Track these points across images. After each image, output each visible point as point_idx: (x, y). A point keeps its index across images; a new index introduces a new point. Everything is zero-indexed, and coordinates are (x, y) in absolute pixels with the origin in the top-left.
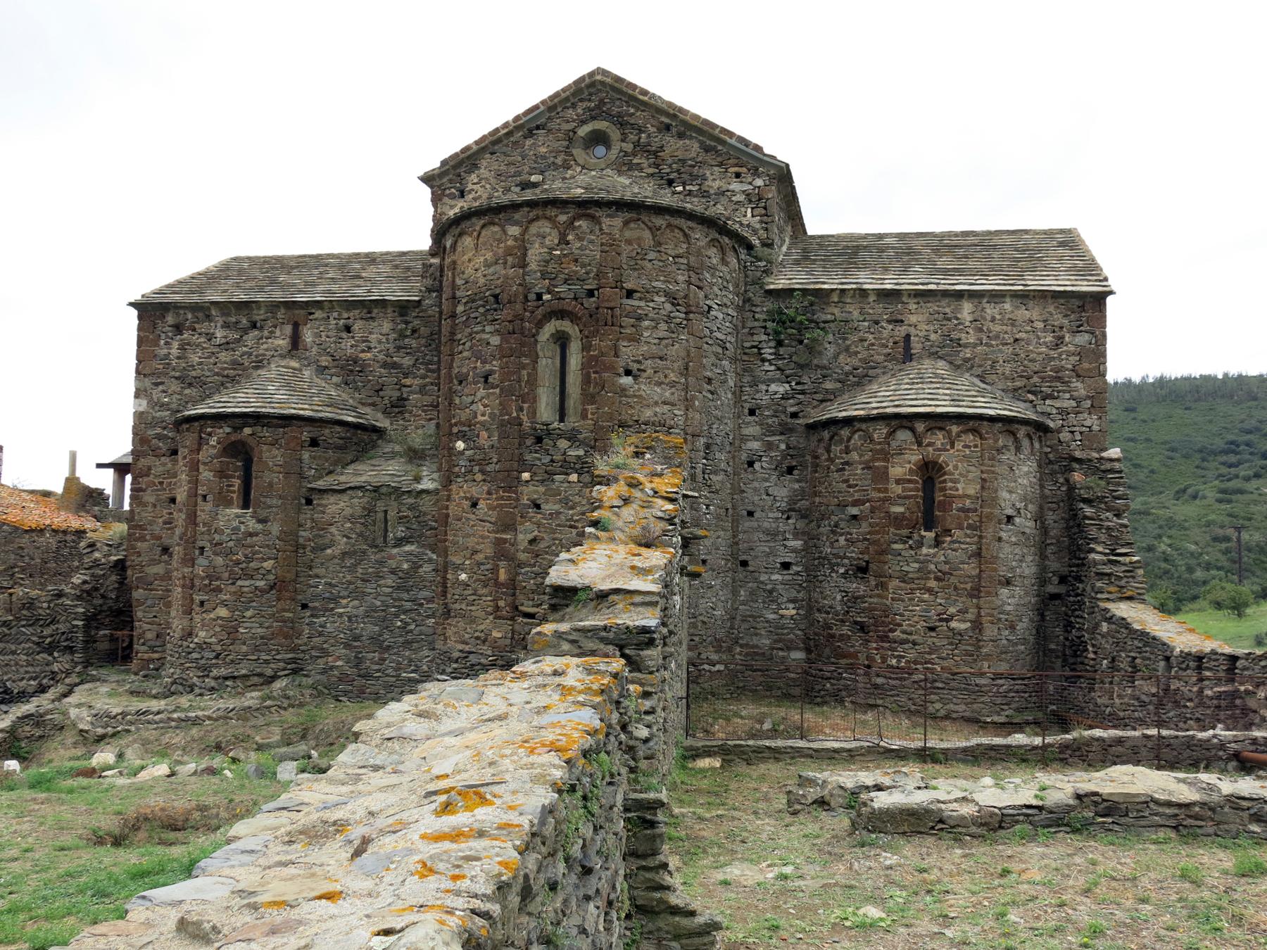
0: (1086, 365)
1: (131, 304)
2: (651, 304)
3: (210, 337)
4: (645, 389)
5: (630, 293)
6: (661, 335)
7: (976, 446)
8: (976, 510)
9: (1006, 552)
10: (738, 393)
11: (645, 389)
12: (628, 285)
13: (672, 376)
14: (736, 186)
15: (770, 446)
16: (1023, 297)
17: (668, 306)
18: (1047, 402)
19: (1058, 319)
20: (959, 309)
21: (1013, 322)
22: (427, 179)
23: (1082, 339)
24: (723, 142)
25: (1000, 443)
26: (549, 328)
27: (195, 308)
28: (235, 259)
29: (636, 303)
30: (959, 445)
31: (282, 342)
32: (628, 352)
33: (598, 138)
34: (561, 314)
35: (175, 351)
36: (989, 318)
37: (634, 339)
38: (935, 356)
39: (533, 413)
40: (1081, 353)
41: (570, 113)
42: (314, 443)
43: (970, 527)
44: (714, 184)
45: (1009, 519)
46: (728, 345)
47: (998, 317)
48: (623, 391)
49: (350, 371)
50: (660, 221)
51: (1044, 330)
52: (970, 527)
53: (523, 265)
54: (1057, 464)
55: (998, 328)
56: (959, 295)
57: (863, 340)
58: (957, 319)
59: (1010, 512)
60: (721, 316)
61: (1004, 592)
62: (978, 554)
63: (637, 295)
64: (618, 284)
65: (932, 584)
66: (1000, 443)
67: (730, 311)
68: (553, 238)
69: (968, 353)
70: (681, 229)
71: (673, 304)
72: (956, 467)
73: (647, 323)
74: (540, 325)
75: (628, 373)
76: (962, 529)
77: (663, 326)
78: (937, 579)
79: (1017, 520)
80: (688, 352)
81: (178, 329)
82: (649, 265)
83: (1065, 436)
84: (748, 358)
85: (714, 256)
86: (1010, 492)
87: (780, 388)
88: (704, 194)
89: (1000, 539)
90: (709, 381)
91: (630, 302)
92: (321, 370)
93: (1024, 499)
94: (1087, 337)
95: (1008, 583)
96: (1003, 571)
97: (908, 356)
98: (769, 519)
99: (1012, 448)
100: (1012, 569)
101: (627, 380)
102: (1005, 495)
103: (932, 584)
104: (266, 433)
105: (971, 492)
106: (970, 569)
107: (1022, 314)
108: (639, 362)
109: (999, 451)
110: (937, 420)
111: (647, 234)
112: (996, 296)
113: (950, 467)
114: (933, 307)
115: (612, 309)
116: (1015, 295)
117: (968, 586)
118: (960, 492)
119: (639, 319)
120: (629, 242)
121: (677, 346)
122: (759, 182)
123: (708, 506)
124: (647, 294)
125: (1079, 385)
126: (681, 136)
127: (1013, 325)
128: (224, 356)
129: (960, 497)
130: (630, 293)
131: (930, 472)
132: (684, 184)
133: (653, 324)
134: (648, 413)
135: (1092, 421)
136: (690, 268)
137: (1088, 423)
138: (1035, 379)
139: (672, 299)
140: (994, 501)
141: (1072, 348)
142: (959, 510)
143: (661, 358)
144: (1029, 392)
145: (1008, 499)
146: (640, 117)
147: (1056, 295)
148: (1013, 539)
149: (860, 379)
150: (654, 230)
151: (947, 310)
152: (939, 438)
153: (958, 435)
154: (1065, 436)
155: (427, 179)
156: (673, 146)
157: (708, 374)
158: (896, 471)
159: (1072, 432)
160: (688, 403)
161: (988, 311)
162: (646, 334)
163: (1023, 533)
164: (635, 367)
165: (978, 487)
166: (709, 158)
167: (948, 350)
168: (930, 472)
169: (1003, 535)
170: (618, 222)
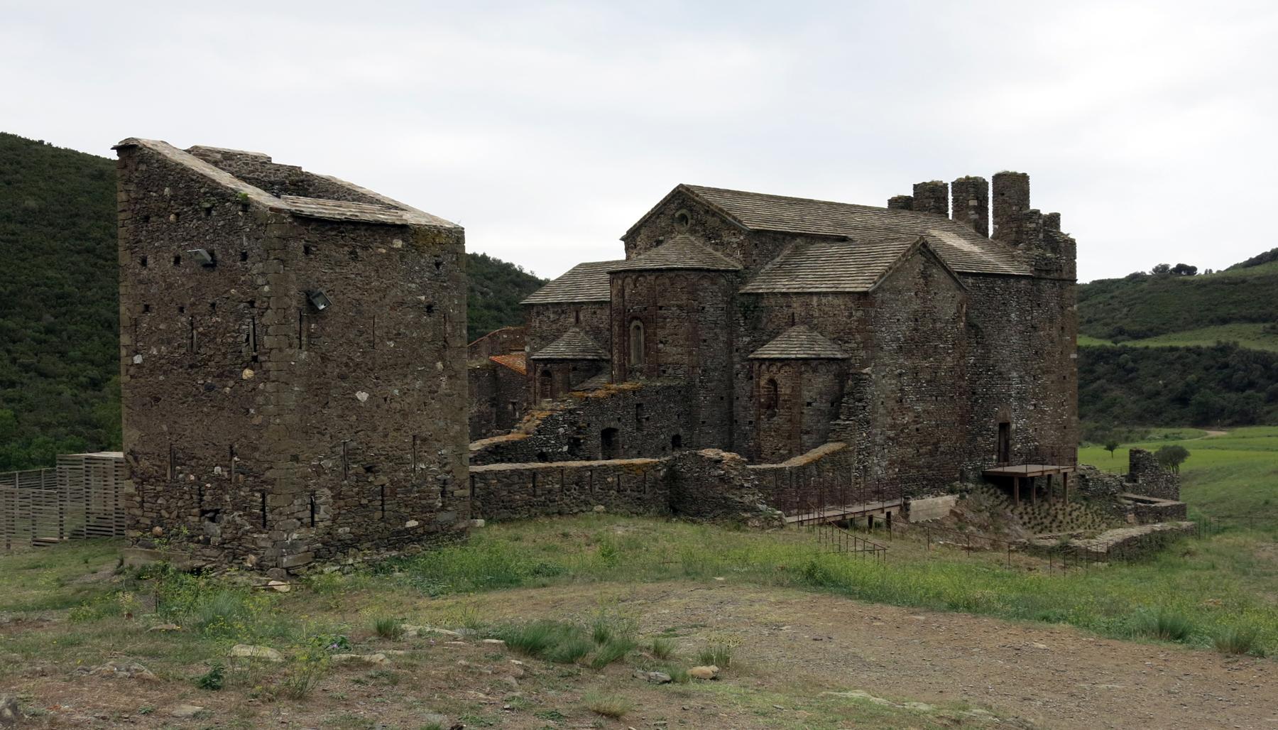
4: (668, 349)
5: (661, 308)
9: (806, 419)
10: (730, 343)
11: (668, 349)
14: (734, 240)
15: (743, 367)
16: (835, 294)
19: (850, 304)
21: (832, 306)
22: (622, 239)
23: (859, 313)
26: (635, 323)
27: (543, 305)
28: (581, 265)
31: (572, 320)
32: (661, 333)
33: (683, 218)
34: (637, 318)
37: (663, 328)
38: (803, 323)
39: (629, 361)
41: (672, 206)
42: (575, 369)
44: (726, 239)
45: (809, 404)
48: (658, 351)
49: (596, 332)
50: (672, 274)
53: (623, 296)
54: (842, 377)
56: (811, 294)
61: (805, 437)
62: (790, 420)
64: (655, 304)
68: (632, 286)
69: (815, 321)
74: (630, 322)
81: (538, 313)
83: (853, 361)
84: (731, 327)
85: (706, 283)
87: (747, 339)
88: (722, 244)
92: (587, 332)
93: (820, 394)
95: (807, 433)
96: (804, 427)
97: (793, 324)
98: (744, 401)
101: (661, 346)
104: (555, 366)
106: (786, 427)
107: (836, 302)
109: (801, 373)
110: (773, 361)
111: (667, 281)
112: (826, 294)
114: (802, 299)
116: (833, 293)
124: (668, 307)
126: (714, 214)
128: (554, 326)
130: (661, 308)
131: (772, 381)
135: (863, 353)
139: (680, 307)
145: (807, 395)
146: (698, 207)
147: (849, 293)
149: (773, 335)
152: (774, 369)
154: (853, 361)
155: (622, 239)
156: (712, 221)
158: (763, 383)
160: (690, 353)
166: (723, 226)
167: (808, 321)
168: (772, 381)
170: (653, 277)
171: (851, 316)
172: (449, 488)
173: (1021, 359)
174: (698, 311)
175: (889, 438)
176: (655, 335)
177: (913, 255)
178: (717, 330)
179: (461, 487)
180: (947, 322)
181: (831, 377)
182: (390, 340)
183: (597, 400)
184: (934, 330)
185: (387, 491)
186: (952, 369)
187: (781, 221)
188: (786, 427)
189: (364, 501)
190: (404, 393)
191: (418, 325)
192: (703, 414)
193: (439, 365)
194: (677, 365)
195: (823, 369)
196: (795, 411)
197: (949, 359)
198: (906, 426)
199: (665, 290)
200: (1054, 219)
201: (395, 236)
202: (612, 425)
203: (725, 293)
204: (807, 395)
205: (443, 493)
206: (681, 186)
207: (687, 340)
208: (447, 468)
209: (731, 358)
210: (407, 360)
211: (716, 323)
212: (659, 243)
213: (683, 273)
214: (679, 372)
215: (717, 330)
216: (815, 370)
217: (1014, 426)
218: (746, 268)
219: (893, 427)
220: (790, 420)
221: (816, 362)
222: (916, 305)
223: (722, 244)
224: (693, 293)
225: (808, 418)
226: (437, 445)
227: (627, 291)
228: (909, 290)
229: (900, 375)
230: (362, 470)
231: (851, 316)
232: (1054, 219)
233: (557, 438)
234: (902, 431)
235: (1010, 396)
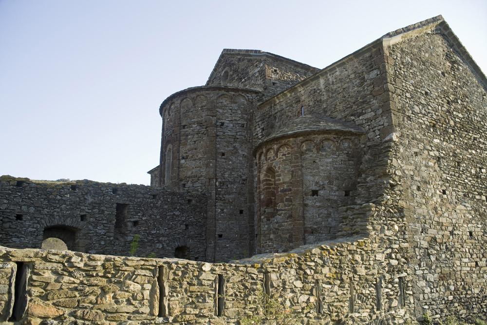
0: (377, 88)
1: (149, 173)
2: (191, 129)
5: (184, 127)
6: (195, 140)
7: (289, 154)
8: (290, 190)
9: (311, 213)
12: (183, 124)
13: (200, 156)
14: (256, 70)
17: (198, 128)
18: (361, 118)
23: (373, 74)
24: (250, 56)
25: (304, 148)
29: (185, 130)
30: (280, 155)
32: (183, 150)
36: (331, 83)
40: (373, 83)
43: (287, 200)
45: (315, 193)
46: (238, 137)
47: (334, 81)
48: (180, 166)
50: (194, 95)
51: (355, 78)
52: (287, 200)
55: (335, 87)
57: (287, 116)
58: (319, 89)
59: (314, 188)
60: (232, 125)
62: (290, 216)
63: (186, 127)
65: (272, 236)
66: (304, 148)
67: (239, 122)
70: (203, 95)
71: (201, 126)
72: (279, 168)
73: (190, 137)
75: (183, 158)
76: (283, 202)
77: (196, 136)
78: (274, 233)
79: (321, 192)
80: (206, 144)
82: (191, 113)
83: (371, 135)
85: (225, 101)
86: (313, 176)
89: (306, 205)
90: (223, 154)
91: (184, 130)
94: (375, 72)
96: (308, 224)
99: (314, 150)
100: (316, 223)
101: (183, 161)
102: (309, 178)
103: (272, 236)
105: (287, 180)
106: (287, 225)
108: (187, 153)
109: (302, 153)
113: (277, 168)
115: (177, 135)
117: (287, 236)
118: (281, 181)
119: (187, 136)
120: (183, 107)
121: (202, 142)
122: (262, 65)
123: (222, 210)
125: (374, 101)
127: (341, 82)
129: (281, 184)
130: (184, 127)
132: (244, 78)
133: (192, 136)
134: (189, 173)
136: (208, 109)
137: (381, 123)
138: (354, 107)
139: (200, 124)
140: (301, 182)
141: (369, 82)
142: (282, 191)
143: (196, 149)
144: (352, 115)
148: (318, 204)
150: (193, 99)
151: (315, 87)
153: (278, 149)
157: (223, 151)
159: (374, 131)
160: (207, 165)
161: (330, 80)
162: (189, 141)
163: (329, 200)
164: (185, 155)
165: (290, 176)
169: (309, 202)
174: (217, 126)
176: (178, 152)
178: (237, 145)
181: (343, 157)
188: (287, 225)
192: (221, 227)
194: (196, 178)
195: (329, 145)
196: (297, 202)
199: (187, 111)
203: (245, 111)
204: (311, 181)
206: (224, 50)
207: (205, 153)
209: (252, 172)
211: (235, 139)
213: (204, 92)
214: (197, 184)
215: (237, 145)
216: (320, 148)
218: (265, 89)
220: (290, 216)
221: (320, 137)
223: (249, 78)
224: (212, 109)
225: (314, 212)
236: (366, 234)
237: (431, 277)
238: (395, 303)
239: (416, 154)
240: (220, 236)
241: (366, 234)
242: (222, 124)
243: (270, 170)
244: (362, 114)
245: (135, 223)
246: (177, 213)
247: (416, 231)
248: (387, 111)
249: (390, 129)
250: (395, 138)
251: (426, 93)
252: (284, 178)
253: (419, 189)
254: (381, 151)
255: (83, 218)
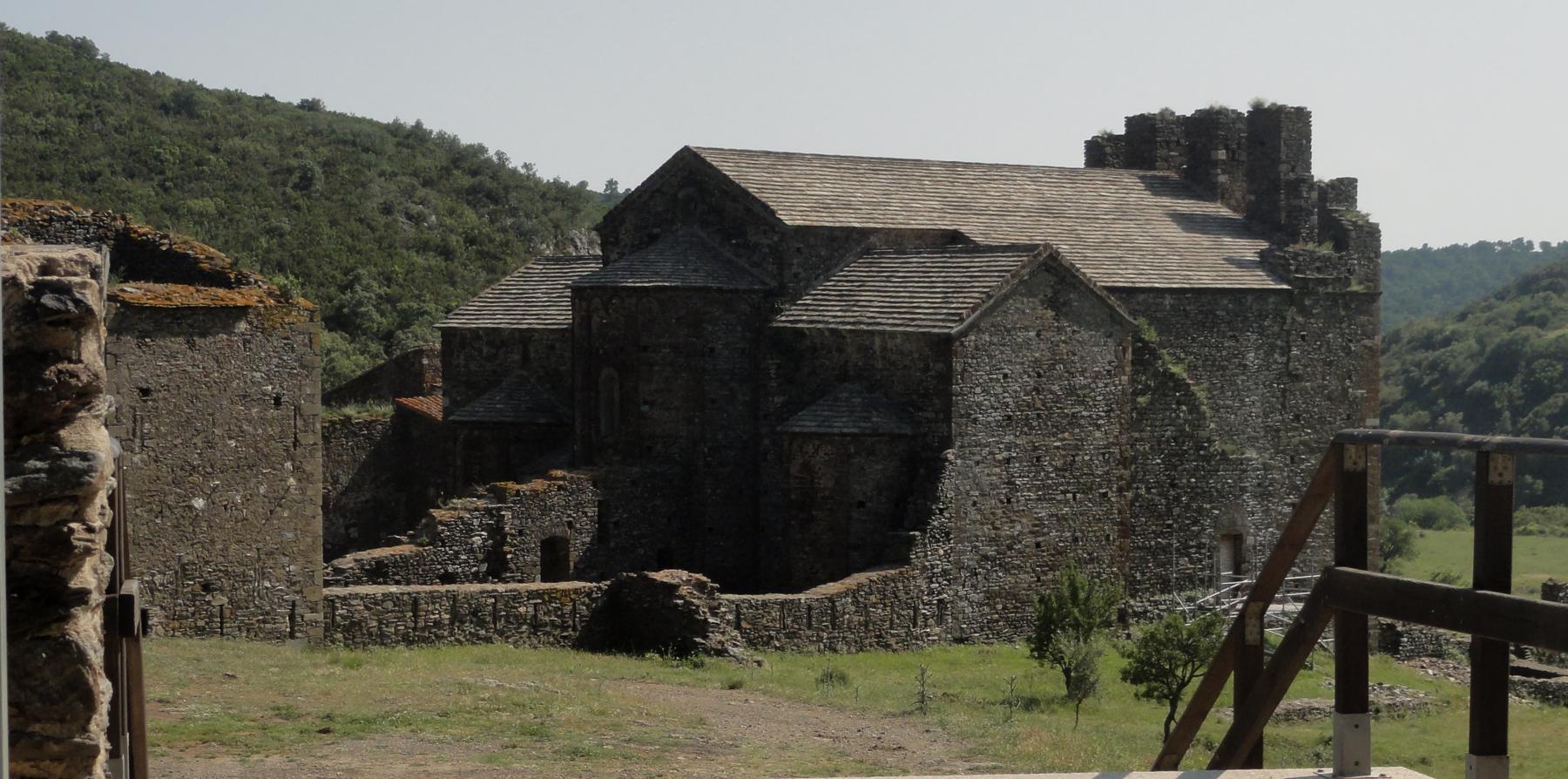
3: (480, 351)
5: (645, 349)
20: (873, 343)
30: (821, 453)
31: (517, 357)
35: (462, 362)
45: (861, 504)
55: (894, 357)
59: (861, 498)
75: (645, 403)
87: (778, 400)
90: (713, 401)
101: (645, 408)
130: (645, 349)
141: (932, 373)
158: (794, 470)
171: (926, 369)
172: (298, 610)
173: (1268, 429)
175: (986, 558)
177: (1032, 274)
179: (313, 610)
180: (1097, 376)
182: (231, 438)
183: (535, 493)
184: (1071, 391)
185: (227, 613)
186: (1104, 451)
187: (848, 206)
189: (201, 623)
190: (246, 500)
191: (263, 420)
193: (288, 465)
197: (1098, 434)
198: (1015, 539)
200: (1345, 189)
201: (238, 319)
202: (558, 531)
205: (292, 617)
208: (297, 588)
210: (251, 461)
212: (653, 239)
217: (1250, 540)
219: (993, 541)
222: (1040, 352)
226: (285, 560)
227: (596, 319)
228: (1026, 329)
229: (1008, 461)
230: (198, 588)
231: (926, 369)
232: (1345, 189)
233: (472, 551)
234: (1010, 548)
235: (1243, 490)
236: (907, 561)
237: (975, 597)
238: (931, 621)
239: (978, 463)
240: (711, 529)
241: (907, 561)
242: (712, 350)
243: (806, 466)
244: (920, 409)
245: (616, 524)
246: (658, 502)
247: (964, 553)
248: (948, 420)
249: (947, 443)
250: (950, 457)
251: (1005, 376)
252: (826, 482)
253: (975, 504)
254: (936, 469)
255: (570, 524)
